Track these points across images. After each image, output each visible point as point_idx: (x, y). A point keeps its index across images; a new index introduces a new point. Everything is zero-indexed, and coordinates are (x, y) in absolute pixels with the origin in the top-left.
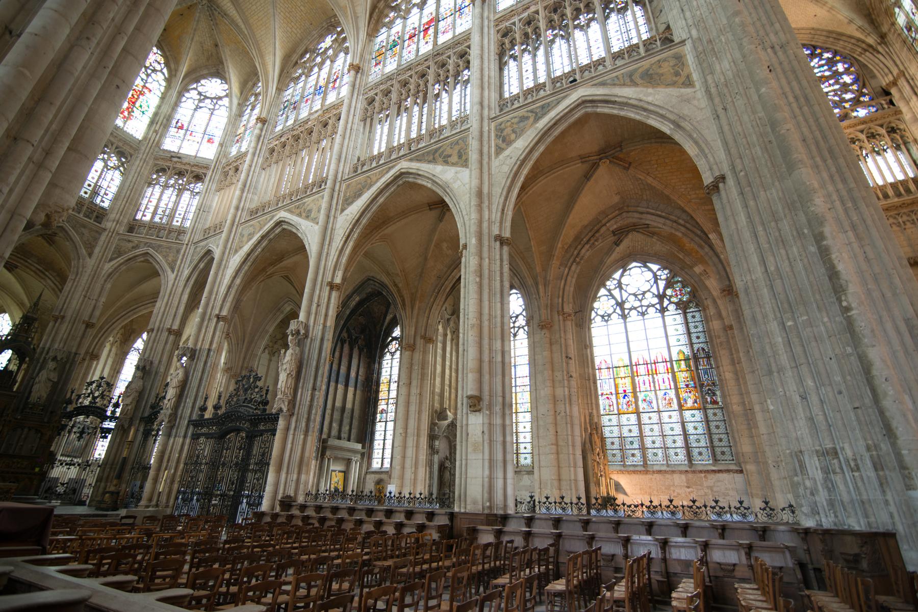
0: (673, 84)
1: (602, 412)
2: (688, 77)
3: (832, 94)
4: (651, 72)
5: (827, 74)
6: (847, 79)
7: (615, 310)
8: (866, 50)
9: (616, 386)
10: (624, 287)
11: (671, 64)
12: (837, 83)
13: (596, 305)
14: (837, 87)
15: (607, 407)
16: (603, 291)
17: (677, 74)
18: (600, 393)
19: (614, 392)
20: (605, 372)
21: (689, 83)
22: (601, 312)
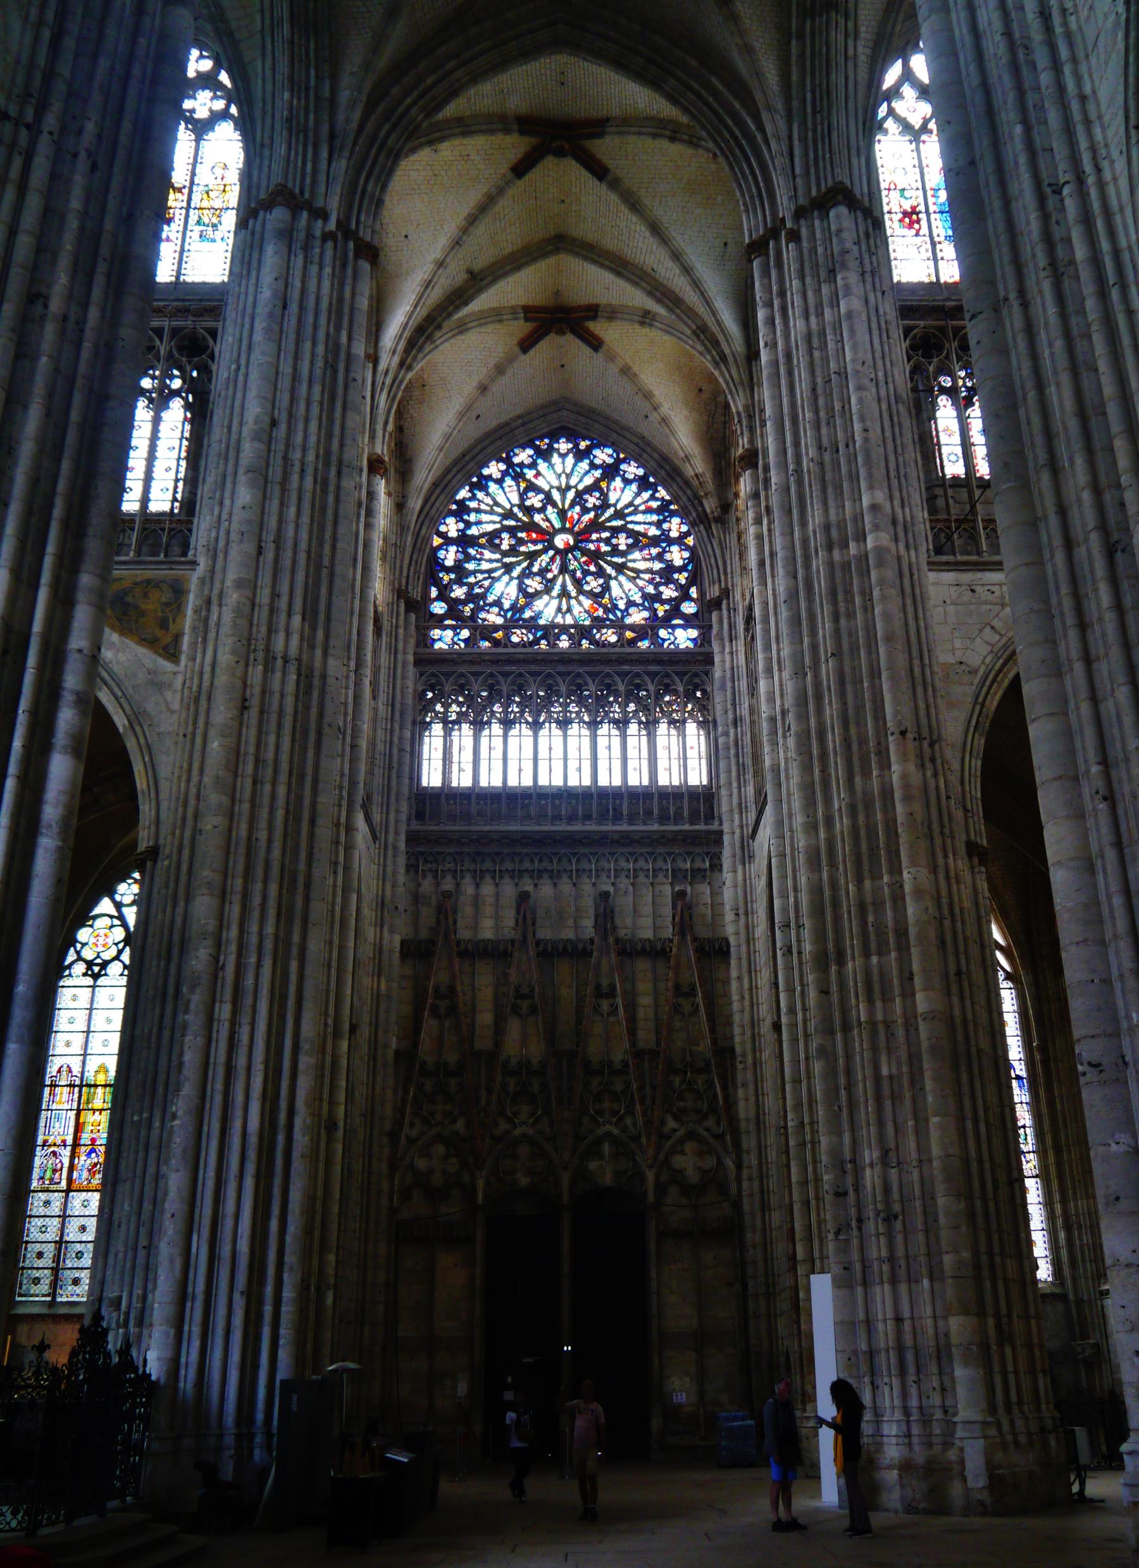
0: (151, 643)
1: (35, 1184)
2: (178, 637)
3: (647, 576)
4: (129, 599)
5: (653, 531)
6: (677, 556)
7: (120, 952)
8: (702, 522)
9: (79, 1128)
10: (116, 922)
11: (164, 600)
12: (660, 557)
13: (83, 934)
14: (657, 566)
15: (48, 1174)
16: (105, 906)
17: (164, 624)
18: (40, 1139)
19: (70, 1141)
20: (62, 1093)
21: (172, 655)
22: (88, 954)
